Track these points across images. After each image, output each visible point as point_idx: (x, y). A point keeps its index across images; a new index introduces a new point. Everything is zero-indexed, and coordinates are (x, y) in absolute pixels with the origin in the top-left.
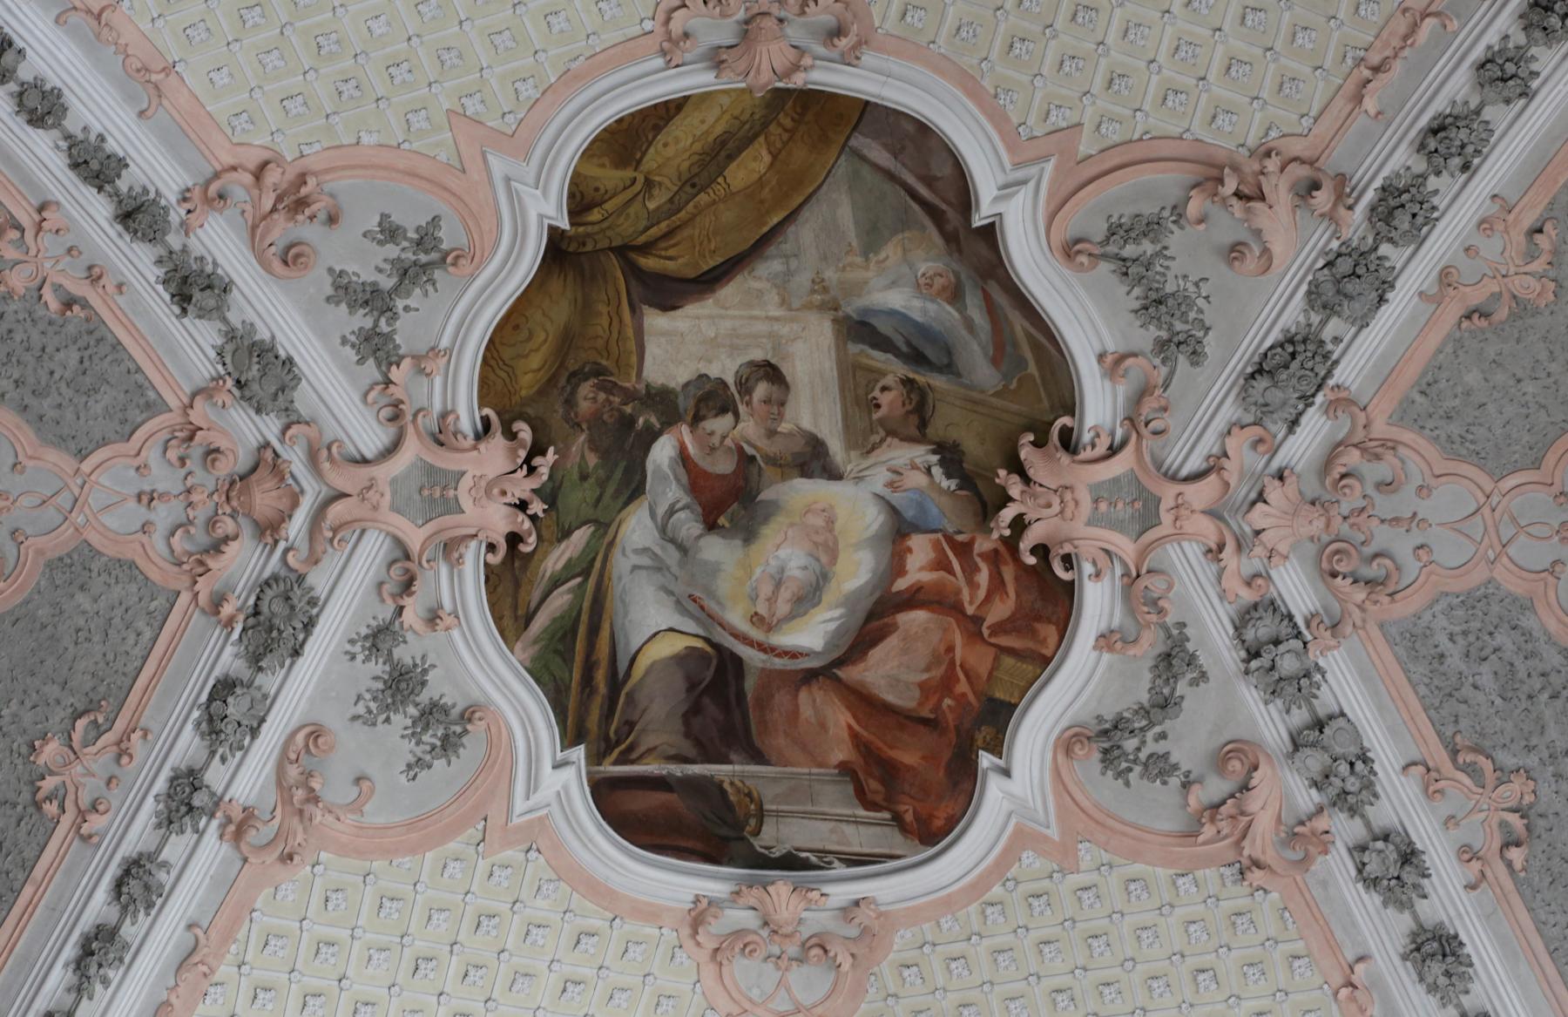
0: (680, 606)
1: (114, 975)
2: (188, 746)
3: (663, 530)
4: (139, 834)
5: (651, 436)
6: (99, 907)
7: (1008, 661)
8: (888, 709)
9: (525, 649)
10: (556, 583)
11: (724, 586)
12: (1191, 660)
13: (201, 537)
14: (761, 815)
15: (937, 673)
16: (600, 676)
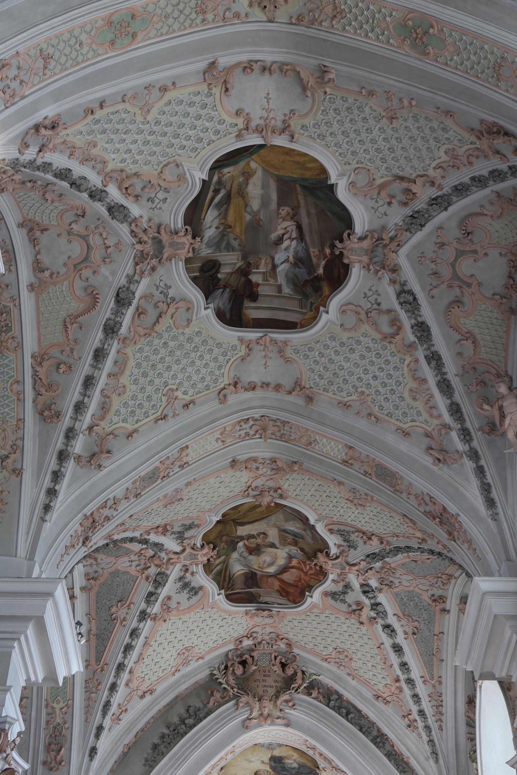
0: (244, 566)
1: (131, 652)
2: (143, 606)
3: (240, 555)
4: (134, 624)
5: (238, 542)
6: (127, 640)
7: (312, 580)
8: (287, 583)
9: (211, 576)
10: (218, 565)
11: (253, 563)
12: (351, 588)
13: (142, 566)
14: (260, 596)
15: (298, 579)
16: (227, 578)
